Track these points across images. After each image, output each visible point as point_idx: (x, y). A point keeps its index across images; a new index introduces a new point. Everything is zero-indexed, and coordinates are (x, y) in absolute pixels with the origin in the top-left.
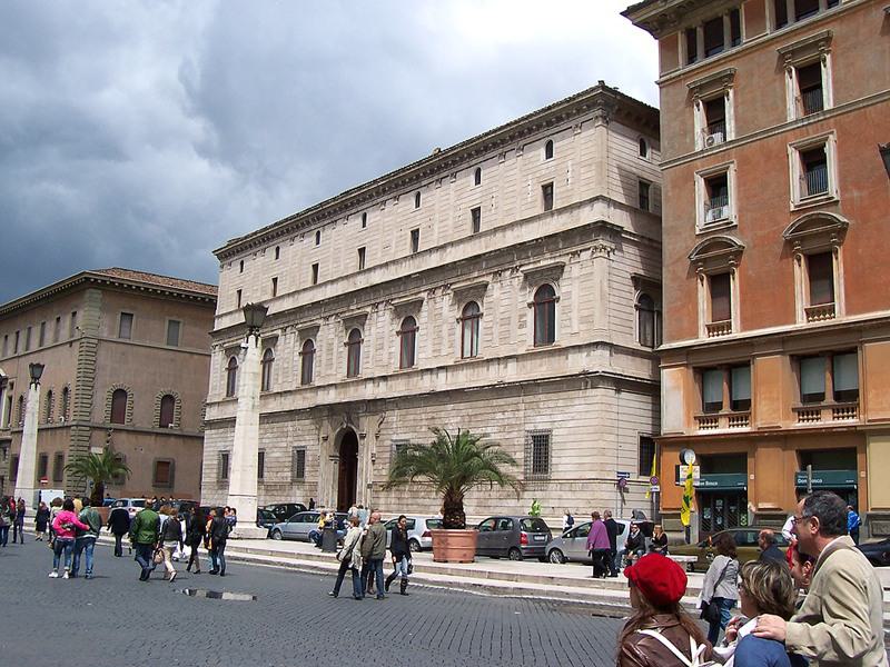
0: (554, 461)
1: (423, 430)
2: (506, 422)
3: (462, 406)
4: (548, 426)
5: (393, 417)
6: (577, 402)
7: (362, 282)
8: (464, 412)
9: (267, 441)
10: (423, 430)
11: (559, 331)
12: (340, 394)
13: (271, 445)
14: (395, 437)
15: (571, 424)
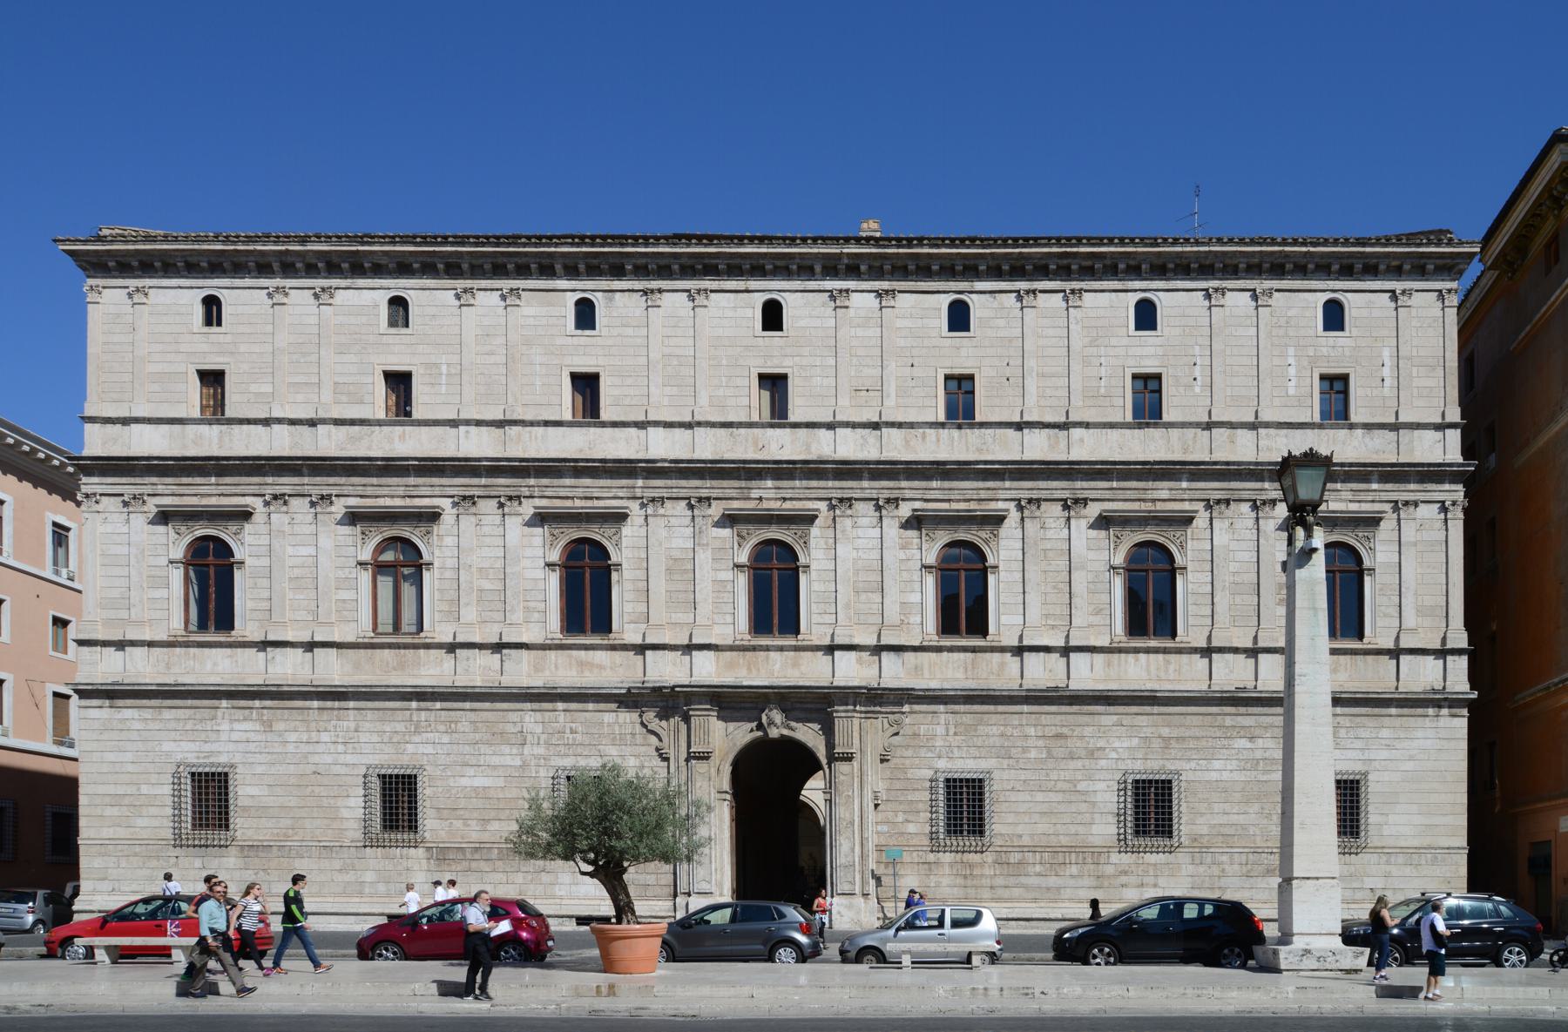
0: (1373, 819)
1: (1033, 754)
2: (1259, 754)
3: (1142, 720)
4: (1359, 767)
5: (936, 724)
6: (1420, 734)
7: (782, 445)
8: (1148, 732)
9: (429, 749)
10: (1033, 754)
11: (1374, 612)
12: (731, 666)
13: (442, 760)
14: (942, 764)
15: (1409, 766)
